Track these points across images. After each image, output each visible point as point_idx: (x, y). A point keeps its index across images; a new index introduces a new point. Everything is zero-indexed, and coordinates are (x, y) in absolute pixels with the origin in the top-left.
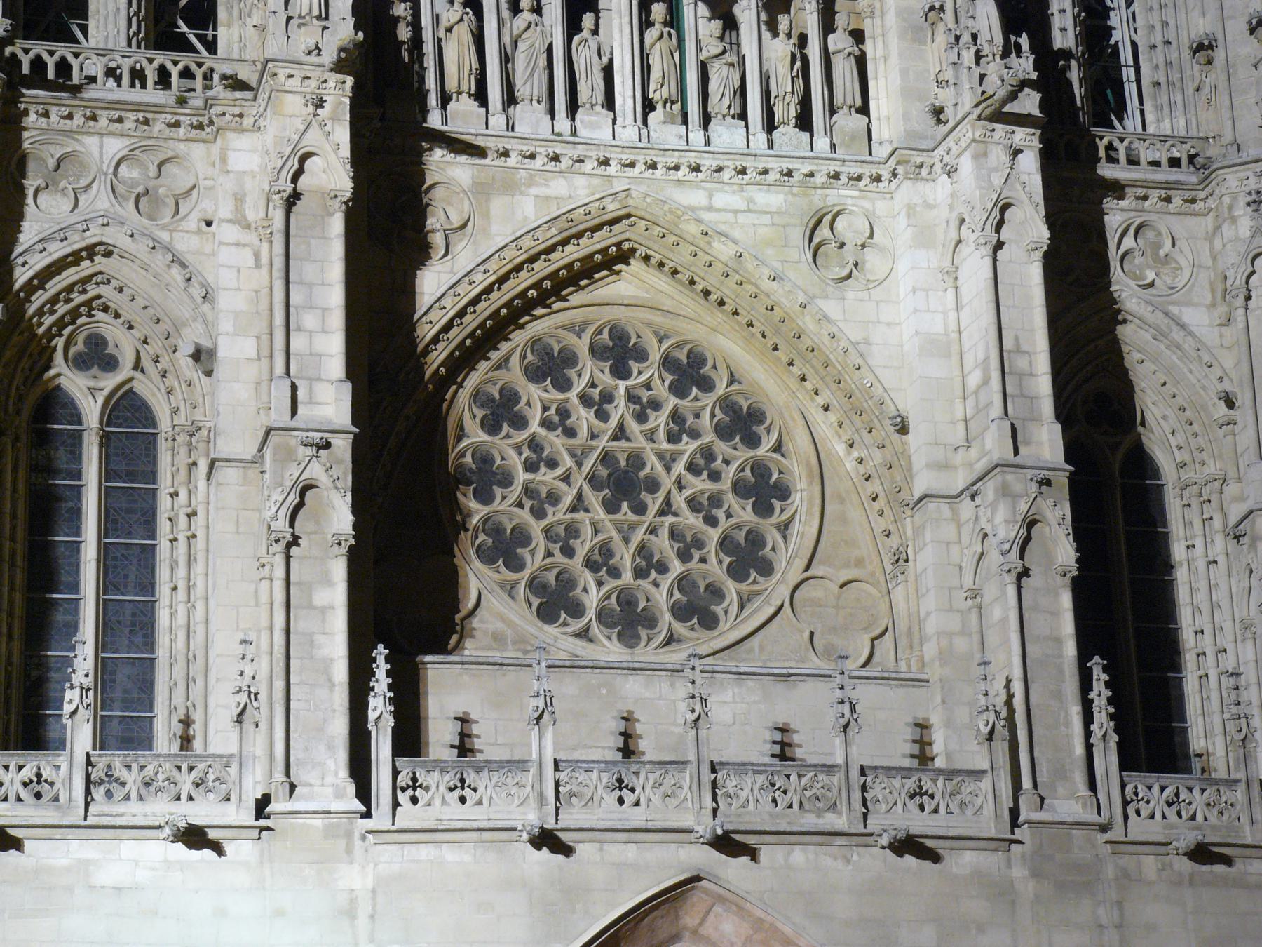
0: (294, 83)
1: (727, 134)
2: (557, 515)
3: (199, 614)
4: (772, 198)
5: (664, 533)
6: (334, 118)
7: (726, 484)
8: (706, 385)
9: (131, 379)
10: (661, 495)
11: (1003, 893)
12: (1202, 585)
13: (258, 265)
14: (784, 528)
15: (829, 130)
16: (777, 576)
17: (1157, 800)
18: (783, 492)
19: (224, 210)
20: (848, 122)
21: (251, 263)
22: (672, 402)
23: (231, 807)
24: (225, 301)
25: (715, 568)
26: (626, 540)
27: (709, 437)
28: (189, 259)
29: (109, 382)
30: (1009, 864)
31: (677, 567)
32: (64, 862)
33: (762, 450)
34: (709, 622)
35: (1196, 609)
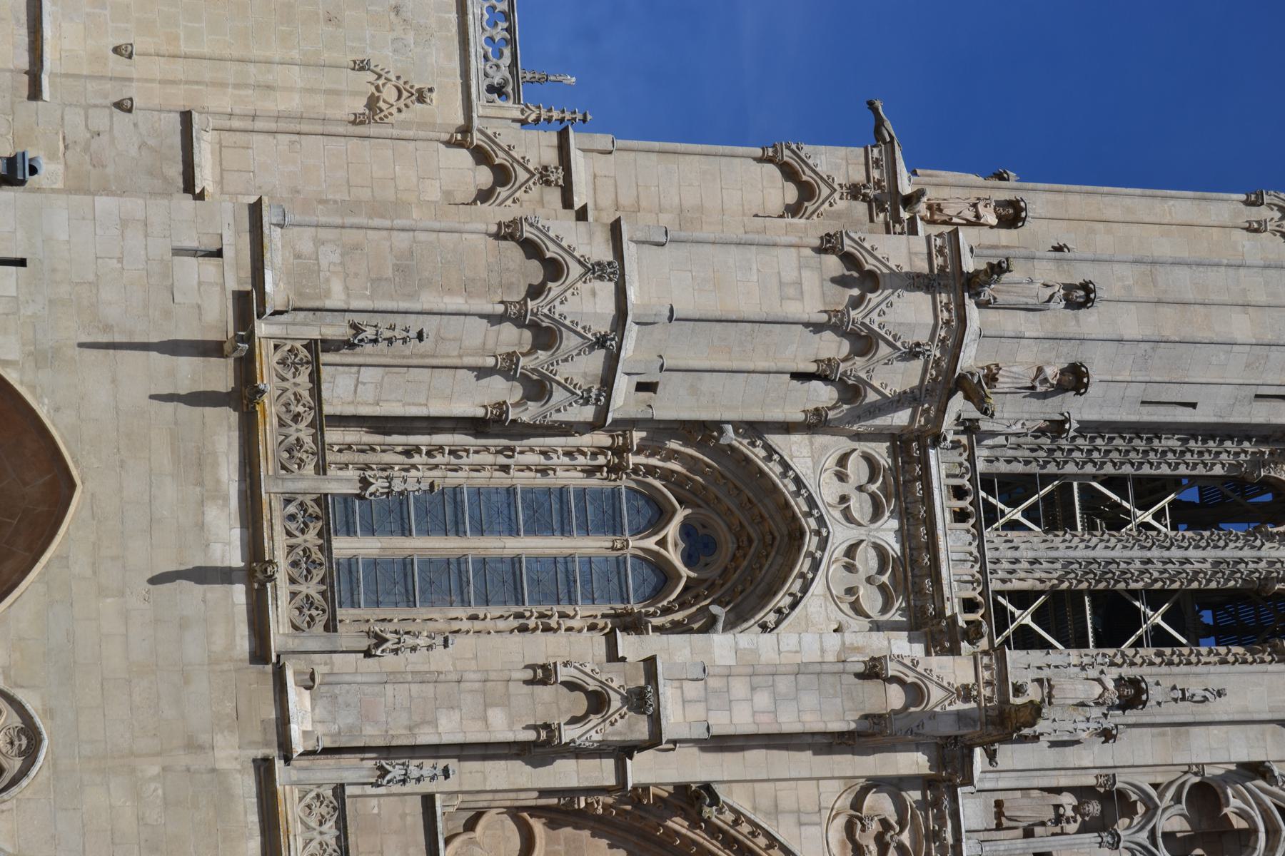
0: (986, 675)
19: (849, 637)
23: (285, 628)
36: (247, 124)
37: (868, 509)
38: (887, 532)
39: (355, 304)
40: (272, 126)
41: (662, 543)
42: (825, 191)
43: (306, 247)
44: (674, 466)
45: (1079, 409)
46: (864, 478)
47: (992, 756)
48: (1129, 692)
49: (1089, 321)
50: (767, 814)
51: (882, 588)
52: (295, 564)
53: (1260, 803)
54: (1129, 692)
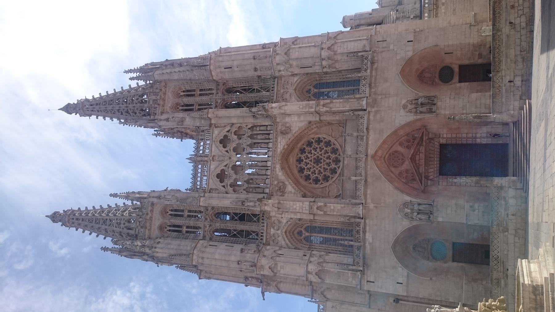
0: (263, 207)
1: (270, 145)
2: (322, 170)
3: (335, 222)
4: (279, 139)
6: (268, 202)
7: (318, 147)
8: (304, 149)
11: (376, 112)
12: (334, 78)
13: (288, 212)
14: (324, 138)
15: (270, 130)
17: (363, 88)
18: (319, 138)
19: (280, 216)
20: (269, 128)
23: (361, 223)
24: (292, 217)
25: (329, 149)
27: (312, 149)
28: (287, 221)
29: (304, 232)
30: (372, 111)
31: (329, 154)
32: (369, 246)
33: (314, 141)
34: (337, 149)
35: (337, 78)
36: (361, 305)
38: (272, 231)
40: (357, 305)
42: (274, 285)
43: (354, 282)
44: (302, 245)
46: (275, 240)
47: (264, 197)
48: (244, 203)
49: (239, 259)
51: (275, 224)
52: (359, 232)
54: (244, 203)
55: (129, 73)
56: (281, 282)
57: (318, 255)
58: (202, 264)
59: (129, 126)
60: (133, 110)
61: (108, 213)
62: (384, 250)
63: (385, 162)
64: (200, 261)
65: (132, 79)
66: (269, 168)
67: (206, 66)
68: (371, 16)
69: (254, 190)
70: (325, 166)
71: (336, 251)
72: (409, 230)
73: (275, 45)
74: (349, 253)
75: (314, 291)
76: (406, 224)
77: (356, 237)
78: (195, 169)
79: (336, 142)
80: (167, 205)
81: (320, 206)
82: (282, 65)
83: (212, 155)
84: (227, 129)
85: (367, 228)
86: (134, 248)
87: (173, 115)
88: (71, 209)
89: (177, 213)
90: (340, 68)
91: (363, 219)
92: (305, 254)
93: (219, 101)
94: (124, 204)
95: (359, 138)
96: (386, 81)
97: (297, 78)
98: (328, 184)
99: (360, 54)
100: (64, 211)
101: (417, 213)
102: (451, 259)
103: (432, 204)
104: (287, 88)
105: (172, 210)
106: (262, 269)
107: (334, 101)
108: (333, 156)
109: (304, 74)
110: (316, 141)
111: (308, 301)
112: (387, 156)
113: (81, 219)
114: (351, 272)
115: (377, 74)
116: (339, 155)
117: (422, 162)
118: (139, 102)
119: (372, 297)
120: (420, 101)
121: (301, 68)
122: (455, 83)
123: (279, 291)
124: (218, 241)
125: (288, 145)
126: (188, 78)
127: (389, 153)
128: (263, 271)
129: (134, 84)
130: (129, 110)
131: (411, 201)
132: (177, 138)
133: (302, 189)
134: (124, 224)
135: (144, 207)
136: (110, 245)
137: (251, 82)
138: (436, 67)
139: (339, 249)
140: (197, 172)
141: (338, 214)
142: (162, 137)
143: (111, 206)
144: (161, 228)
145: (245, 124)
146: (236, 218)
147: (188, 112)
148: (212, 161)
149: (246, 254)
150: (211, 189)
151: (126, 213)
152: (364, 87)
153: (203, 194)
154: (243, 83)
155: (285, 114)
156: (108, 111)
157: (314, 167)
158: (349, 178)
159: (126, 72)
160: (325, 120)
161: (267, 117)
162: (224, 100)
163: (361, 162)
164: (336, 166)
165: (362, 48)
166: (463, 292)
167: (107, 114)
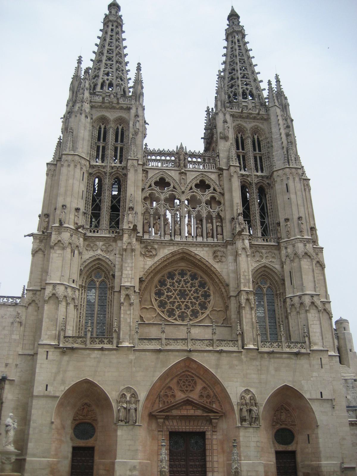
1: (200, 239)
2: (171, 300)
5: (189, 303)
6: (133, 237)
8: (197, 279)
9: (103, 279)
10: (188, 297)
11: (241, 360)
14: (209, 302)
15: (217, 237)
16: (208, 310)
18: (209, 296)
19: (117, 252)
20: (219, 236)
21: (121, 260)
22: (191, 282)
24: (116, 266)
26: (183, 304)
30: (242, 355)
33: (205, 290)
34: (197, 317)
35: (279, 315)
37: (95, 247)
39: (58, 329)
41: (98, 281)
43: (47, 337)
44: (85, 277)
45: (82, 209)
47: (139, 233)
48: (131, 209)
49: (68, 206)
50: (144, 269)
51: (109, 246)
52: (101, 343)
53: (147, 191)
54: (131, 209)
55: (275, 80)
56: (44, 255)
57: (74, 297)
58: (62, 165)
59: (217, 81)
60: (234, 85)
61: (120, 62)
62: (83, 371)
63: (183, 372)
64: (66, 164)
65: (269, 83)
66: (173, 238)
67: (289, 163)
68: (349, 351)
69: (147, 221)
70: (177, 304)
71: (80, 317)
72: (107, 399)
73: (315, 242)
74: (77, 332)
75: (34, 292)
76: (113, 395)
77: (96, 340)
78: (170, 154)
79: (205, 315)
80: (129, 124)
81: (130, 299)
82: (293, 251)
83: (186, 172)
84: (217, 188)
85: (107, 352)
86: (81, 91)
87: (230, 127)
88: (123, 23)
89: (120, 135)
90: (291, 317)
91: (117, 347)
92: (75, 282)
93: (249, 179)
94: (130, 79)
95: (211, 342)
96: (277, 370)
97: (278, 269)
98: (156, 308)
99: (307, 339)
100: (121, 16)
101: (126, 407)
102: (75, 445)
103: (137, 424)
104: (267, 256)
105: (122, 129)
106: (57, 233)
107: (253, 312)
108: (188, 313)
109: (283, 276)
110: (205, 292)
111: (24, 286)
112: (190, 374)
113: (112, 34)
114: (57, 334)
115: (285, 359)
116: (190, 320)
117: (184, 413)
118: (244, 91)
119: (31, 357)
120: (255, 408)
121: (290, 272)
122: (275, 447)
123: (35, 253)
124: (88, 183)
125: (199, 261)
126: (273, 144)
127: (193, 376)
128: (55, 234)
129: (264, 85)
130: (234, 81)
131: (139, 401)
132: (204, 133)
133: (150, 277)
134: (108, 80)
135: (127, 100)
136: (84, 66)
137: (273, 215)
138: (293, 425)
139: (82, 321)
140: (166, 155)
141: (122, 319)
142: (206, 117)
143: (127, 65)
144: (103, 120)
145: (223, 209)
146: (114, 202)
147: (235, 146)
148: (179, 172)
149: (74, 213)
150: (147, 172)
151: (120, 80)
152: (270, 345)
153: (141, 163)
154: (271, 205)
155: (236, 255)
156: (232, 58)
157: (175, 290)
158: (163, 332)
159: (277, 77)
160: (230, 302)
161: (233, 234)
162: (251, 184)
163: (182, 344)
164: (177, 316)
165: (314, 341)
166: (40, 457)
167: (229, 57)
